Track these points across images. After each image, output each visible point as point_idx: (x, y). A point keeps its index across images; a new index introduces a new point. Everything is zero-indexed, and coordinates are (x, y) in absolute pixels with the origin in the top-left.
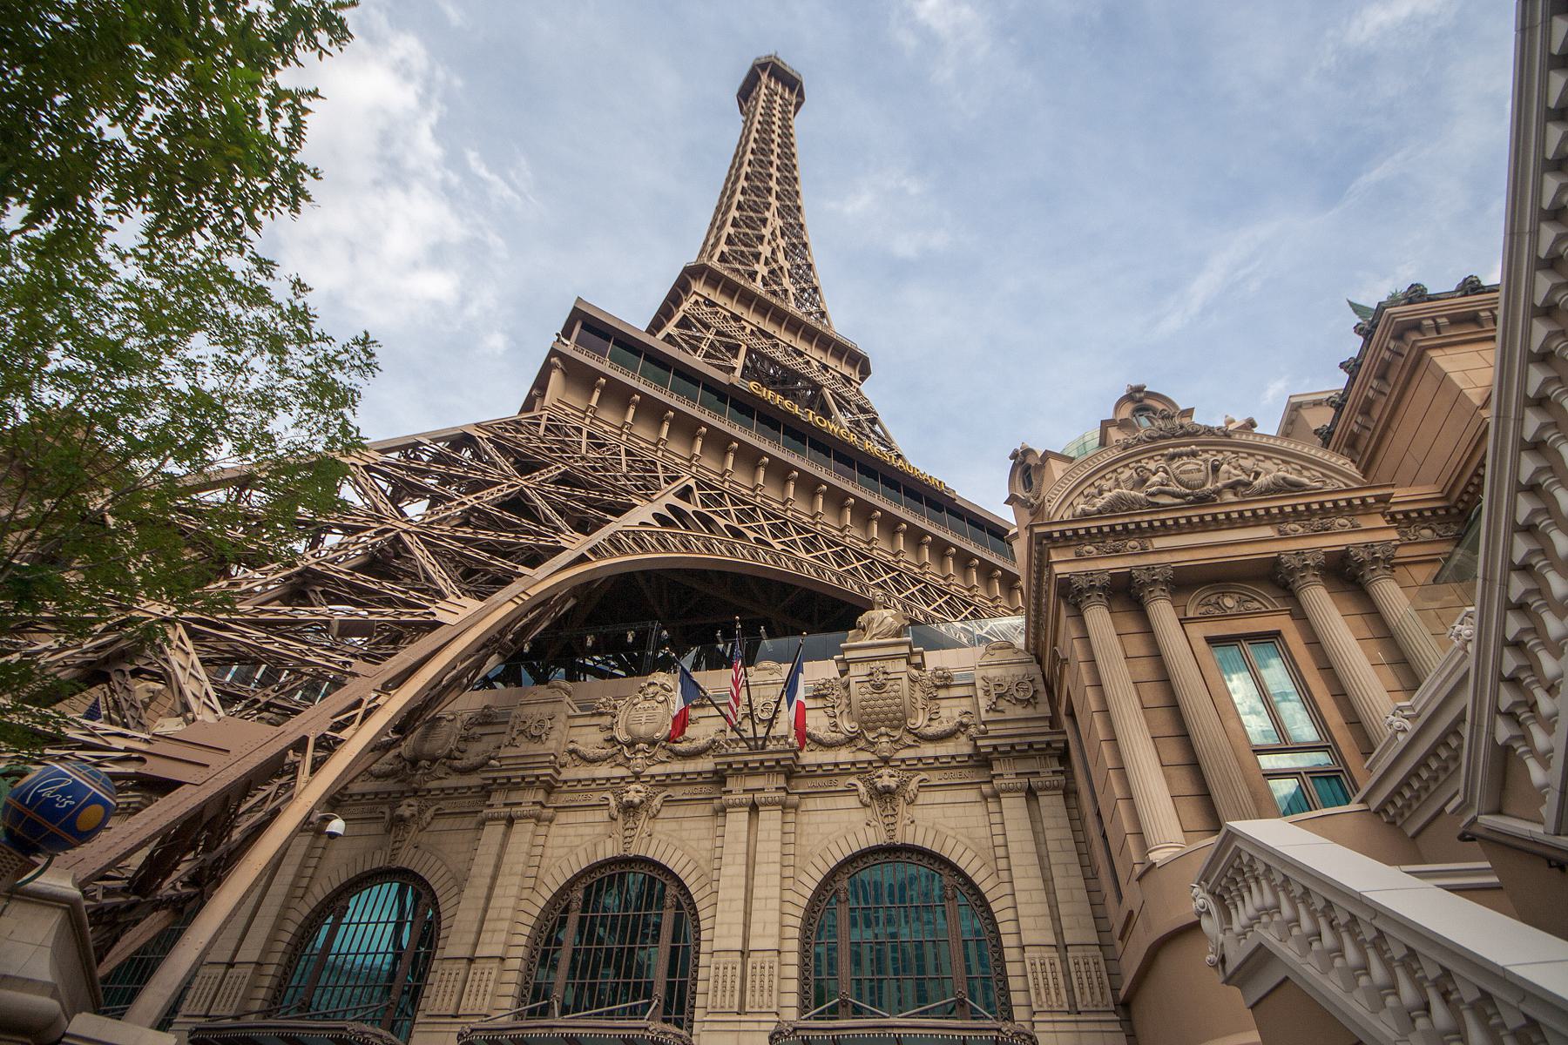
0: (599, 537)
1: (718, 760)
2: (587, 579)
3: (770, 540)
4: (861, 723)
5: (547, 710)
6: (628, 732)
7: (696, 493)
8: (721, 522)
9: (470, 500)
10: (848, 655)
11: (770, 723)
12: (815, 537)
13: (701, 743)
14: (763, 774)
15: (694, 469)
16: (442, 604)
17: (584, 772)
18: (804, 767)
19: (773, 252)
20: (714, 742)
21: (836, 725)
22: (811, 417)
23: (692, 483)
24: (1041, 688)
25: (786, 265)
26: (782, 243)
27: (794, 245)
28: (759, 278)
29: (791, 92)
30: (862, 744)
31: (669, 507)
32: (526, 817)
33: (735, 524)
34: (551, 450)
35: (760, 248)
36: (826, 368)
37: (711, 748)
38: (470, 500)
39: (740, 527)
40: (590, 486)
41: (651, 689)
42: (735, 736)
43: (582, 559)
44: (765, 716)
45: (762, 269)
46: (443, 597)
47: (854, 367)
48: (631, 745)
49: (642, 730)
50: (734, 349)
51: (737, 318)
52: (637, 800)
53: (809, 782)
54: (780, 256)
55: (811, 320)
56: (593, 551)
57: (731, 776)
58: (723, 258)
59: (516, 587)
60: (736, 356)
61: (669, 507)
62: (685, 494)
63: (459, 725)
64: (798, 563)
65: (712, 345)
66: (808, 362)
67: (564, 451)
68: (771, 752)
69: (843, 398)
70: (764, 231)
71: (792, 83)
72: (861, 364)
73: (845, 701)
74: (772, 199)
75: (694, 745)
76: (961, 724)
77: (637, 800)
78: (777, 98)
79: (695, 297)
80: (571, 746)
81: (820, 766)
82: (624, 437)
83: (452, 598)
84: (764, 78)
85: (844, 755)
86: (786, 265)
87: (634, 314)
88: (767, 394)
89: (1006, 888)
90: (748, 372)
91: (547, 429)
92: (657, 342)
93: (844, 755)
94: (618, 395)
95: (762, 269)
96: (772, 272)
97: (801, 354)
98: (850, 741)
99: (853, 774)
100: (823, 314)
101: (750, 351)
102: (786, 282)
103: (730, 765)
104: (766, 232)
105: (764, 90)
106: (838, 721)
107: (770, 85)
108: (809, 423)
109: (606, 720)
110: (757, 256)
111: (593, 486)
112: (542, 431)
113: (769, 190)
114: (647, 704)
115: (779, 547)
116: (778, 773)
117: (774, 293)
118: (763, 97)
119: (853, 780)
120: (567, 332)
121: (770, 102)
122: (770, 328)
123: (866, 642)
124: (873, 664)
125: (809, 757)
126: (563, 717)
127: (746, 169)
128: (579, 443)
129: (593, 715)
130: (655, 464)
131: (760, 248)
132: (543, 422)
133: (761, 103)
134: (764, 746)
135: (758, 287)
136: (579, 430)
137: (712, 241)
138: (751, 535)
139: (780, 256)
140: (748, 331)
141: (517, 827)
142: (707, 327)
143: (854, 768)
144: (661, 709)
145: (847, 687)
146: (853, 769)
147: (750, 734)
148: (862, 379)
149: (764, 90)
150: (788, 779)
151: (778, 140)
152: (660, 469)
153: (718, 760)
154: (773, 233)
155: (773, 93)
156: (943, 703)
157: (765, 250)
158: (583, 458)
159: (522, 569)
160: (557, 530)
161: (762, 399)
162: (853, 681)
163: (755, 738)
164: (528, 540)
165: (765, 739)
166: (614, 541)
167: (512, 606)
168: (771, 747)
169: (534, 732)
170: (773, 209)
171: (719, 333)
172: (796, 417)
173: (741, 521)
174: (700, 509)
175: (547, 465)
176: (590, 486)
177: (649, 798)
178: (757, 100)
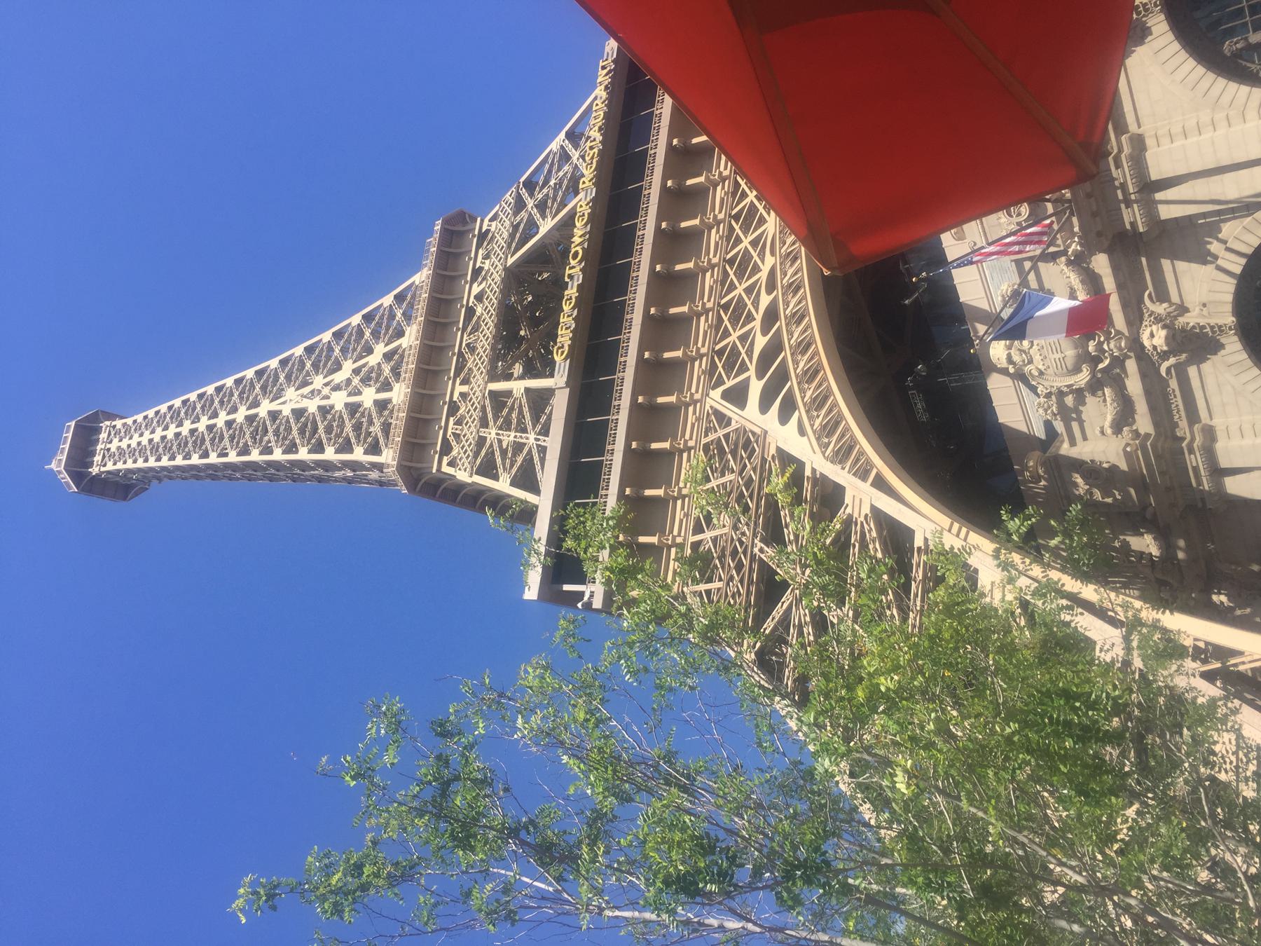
0: (839, 474)
6: (1077, 370)
8: (761, 342)
12: (737, 218)
17: (1141, 407)
19: (337, 388)
22: (575, 272)
23: (716, 394)
26: (318, 381)
31: (764, 406)
33: (757, 324)
34: (739, 567)
35: (339, 406)
37: (1079, 262)
39: (759, 317)
41: (1016, 358)
50: (499, 400)
52: (1163, 333)
54: (339, 377)
56: (863, 474)
58: (374, 449)
60: (509, 393)
65: (507, 426)
67: (735, 553)
69: (512, 236)
77: (1163, 333)
80: (1109, 431)
86: (348, 366)
88: (565, 337)
90: (540, 365)
95: (369, 397)
96: (366, 381)
102: (374, 360)
104: (312, 406)
105: (110, 467)
109: (1069, 400)
110: (353, 409)
112: (716, 585)
114: (1037, 358)
115: (770, 261)
128: (715, 540)
130: (706, 448)
131: (339, 406)
135: (399, 394)
140: (465, 389)
141: (1224, 463)
142: (481, 441)
151: (173, 429)
157: (339, 400)
158: (735, 528)
166: (842, 455)
170: (274, 406)
171: (484, 423)
172: (580, 288)
173: (750, 318)
174: (752, 372)
177: (1158, 319)
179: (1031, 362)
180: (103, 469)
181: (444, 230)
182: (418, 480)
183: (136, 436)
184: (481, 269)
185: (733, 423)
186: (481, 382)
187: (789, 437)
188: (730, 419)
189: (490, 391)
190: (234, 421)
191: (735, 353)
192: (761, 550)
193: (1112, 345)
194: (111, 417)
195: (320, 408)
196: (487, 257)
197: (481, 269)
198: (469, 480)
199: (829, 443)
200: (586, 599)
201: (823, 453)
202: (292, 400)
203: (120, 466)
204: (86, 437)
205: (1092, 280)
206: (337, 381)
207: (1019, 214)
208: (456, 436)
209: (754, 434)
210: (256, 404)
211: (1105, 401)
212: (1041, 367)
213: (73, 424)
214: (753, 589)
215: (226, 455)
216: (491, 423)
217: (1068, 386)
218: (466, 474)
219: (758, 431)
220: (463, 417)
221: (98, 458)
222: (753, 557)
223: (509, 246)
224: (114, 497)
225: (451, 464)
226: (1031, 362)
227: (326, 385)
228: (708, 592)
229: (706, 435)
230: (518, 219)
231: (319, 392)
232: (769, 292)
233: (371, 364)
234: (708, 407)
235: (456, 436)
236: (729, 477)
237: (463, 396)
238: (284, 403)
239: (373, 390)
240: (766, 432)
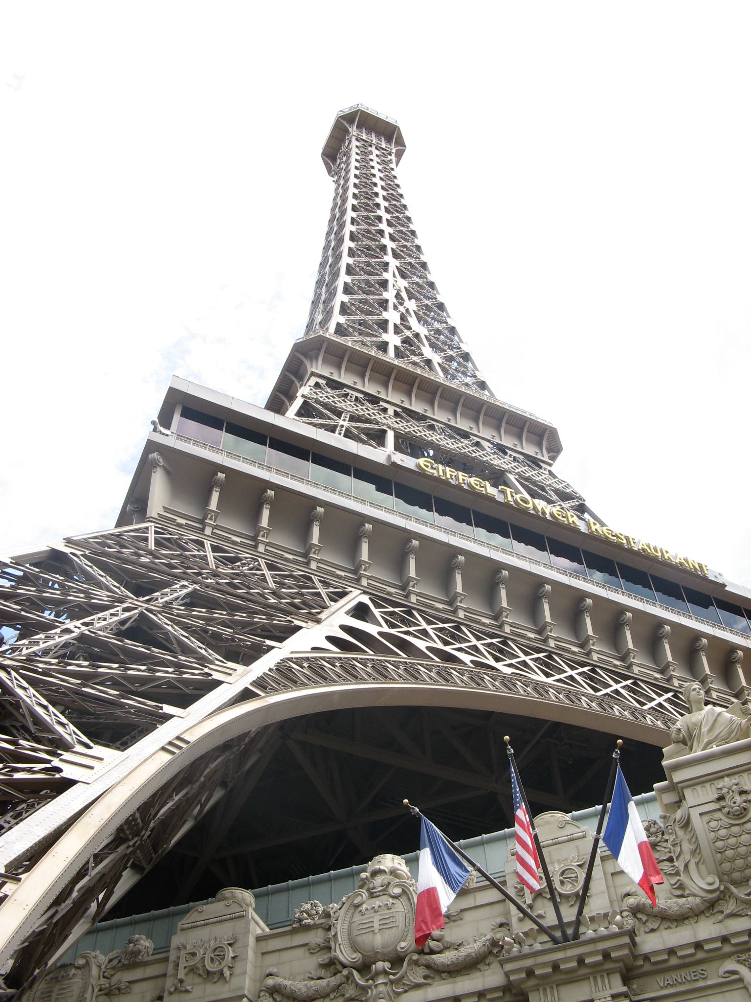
1: (508, 967)
2: (254, 727)
3: (491, 662)
4: (721, 875)
5: (224, 931)
6: (355, 948)
7: (376, 612)
8: (421, 644)
9: (76, 627)
10: (678, 777)
11: (582, 898)
13: (473, 948)
14: (586, 978)
15: (364, 582)
16: (66, 756)
18: (646, 957)
19: (403, 318)
20: (494, 943)
21: (681, 887)
23: (365, 599)
25: (423, 331)
26: (411, 305)
27: (428, 308)
29: (389, 140)
30: (731, 907)
31: (345, 628)
33: (439, 645)
35: (385, 315)
36: (502, 449)
37: (493, 951)
38: (76, 627)
39: (448, 649)
40: (233, 608)
41: (379, 880)
42: (529, 925)
43: (246, 695)
44: (567, 889)
45: (393, 340)
46: (68, 748)
47: (539, 445)
48: (364, 968)
49: (378, 941)
51: (374, 400)
53: (660, 980)
55: (474, 392)
56: (261, 683)
57: (536, 988)
58: (340, 330)
59: (163, 734)
61: (344, 628)
62: (361, 612)
63: (95, 971)
64: (539, 688)
66: (477, 444)
68: (593, 941)
69: (535, 483)
70: (385, 295)
71: (389, 133)
72: (545, 438)
73: (687, 847)
74: (389, 258)
75: (463, 952)
78: (373, 149)
79: (313, 381)
80: (270, 982)
81: (671, 952)
82: (261, 548)
83: (79, 748)
84: (353, 130)
85: (706, 929)
86: (423, 331)
87: (250, 395)
91: (158, 543)
92: (289, 421)
93: (706, 929)
94: (247, 495)
95: (393, 340)
97: (465, 435)
98: (711, 906)
99: (728, 956)
100: (482, 385)
101: (397, 436)
102: (427, 351)
103: (530, 973)
104: (389, 295)
105: (355, 143)
106: (683, 878)
107: (360, 138)
108: (506, 505)
109: (316, 938)
110: (383, 325)
111: (239, 608)
112: (152, 545)
113: (383, 248)
114: (377, 903)
116: (609, 973)
117: (415, 364)
118: (354, 150)
119: (730, 965)
120: (165, 419)
121: (364, 154)
122: (418, 407)
123: (698, 753)
124: (720, 784)
125: (653, 942)
126: (252, 941)
127: (349, 228)
129: (294, 931)
130: (310, 579)
131: (385, 315)
132: (151, 537)
133: (354, 157)
134: (576, 936)
136: (201, 544)
137: (319, 318)
138: (466, 658)
139: (413, 321)
140: (391, 412)
142: (339, 414)
144: (400, 907)
145: (686, 824)
146: (727, 949)
147: (551, 919)
148: (553, 458)
149: (355, 143)
150: (626, 981)
152: (318, 585)
153: (508, 967)
154: (398, 296)
155: (367, 144)
157: (392, 316)
158: (215, 574)
159: (167, 709)
160: (203, 661)
161: (438, 480)
162: (695, 814)
163: (561, 925)
164: (165, 673)
165: (578, 923)
167: (166, 757)
168: (590, 933)
169: (210, 967)
174: (386, 629)
175: (168, 585)
176: (233, 608)
178: (348, 155)
179: (372, 895)
180: (354, 139)
182: (306, 355)
183: (376, 189)
184: (506, 453)
185: (332, 603)
186: (396, 426)
187: (309, 639)
188: (336, 601)
189: (384, 432)
190: (383, 236)
191: (409, 624)
192: (183, 586)
193: (382, 988)
195: (387, 301)
196: (515, 459)
197: (506, 453)
198: (299, 394)
199: (302, 667)
200: (162, 429)
201: (290, 659)
206: (409, 318)
207: (562, 883)
208: (346, 395)
209: (319, 613)
210: (396, 255)
211: (312, 979)
212: (364, 906)
214: (142, 570)
215: (352, 223)
216: (353, 424)
217: (335, 935)
218: (305, 393)
219: (322, 616)
220: (362, 404)
222: (179, 578)
223: (527, 479)
224: (327, 146)
225: (317, 385)
226: (372, 895)
227: (407, 310)
228: (146, 539)
229: (320, 581)
230: (552, 493)
231: (402, 304)
232: (472, 662)
233: (422, 348)
234: (350, 589)
235: (346, 395)
236: (272, 585)
237: (385, 410)
238: (394, 276)
239: (399, 344)
240: (318, 621)
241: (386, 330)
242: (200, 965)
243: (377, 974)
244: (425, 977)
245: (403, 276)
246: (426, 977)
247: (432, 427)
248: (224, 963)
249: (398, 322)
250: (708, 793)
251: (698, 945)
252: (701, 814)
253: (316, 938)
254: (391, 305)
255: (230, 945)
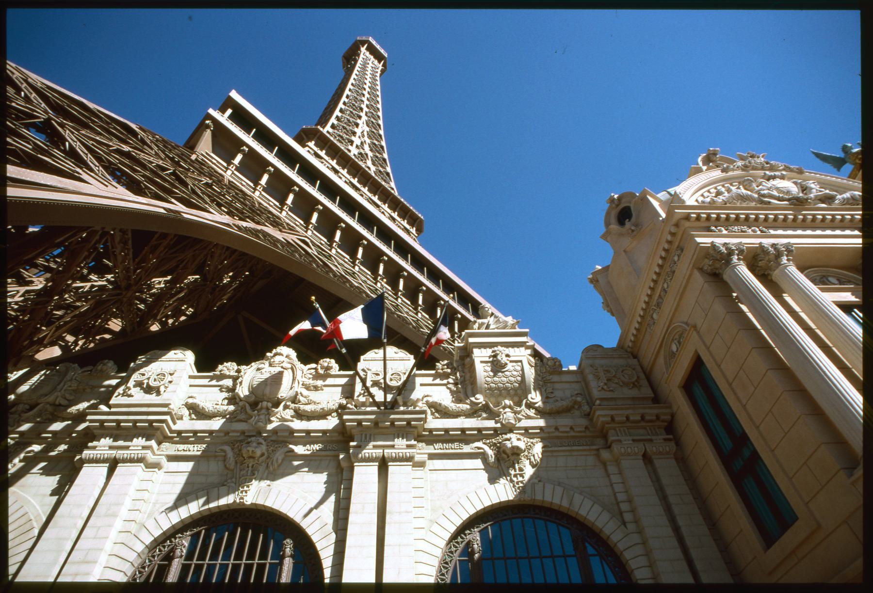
24: (642, 376)
28: (354, 145)
29: (379, 62)
32: (131, 461)
44: (394, 384)
54: (367, 147)
68: (403, 413)
76: (575, 402)
80: (191, 401)
84: (363, 49)
86: (370, 154)
89: (636, 538)
110: (352, 142)
124: (496, 348)
141: (120, 469)
143: (480, 434)
156: (557, 386)
169: (152, 383)
179: (270, 365)
181: (418, 218)
194: (383, 71)
202: (362, 127)
203: (361, 59)
204: (379, 57)
205: (322, 415)
213: (386, 56)
221: (368, 54)
224: (347, 53)
241: (352, 145)
242: (146, 381)
243: (262, 408)
244: (292, 417)
245: (368, 126)
246: (292, 417)
247: (362, 195)
248: (162, 383)
249: (359, 144)
250: (489, 352)
251: (463, 430)
252: (482, 362)
253: (229, 383)
254: (357, 135)
255: (171, 374)
